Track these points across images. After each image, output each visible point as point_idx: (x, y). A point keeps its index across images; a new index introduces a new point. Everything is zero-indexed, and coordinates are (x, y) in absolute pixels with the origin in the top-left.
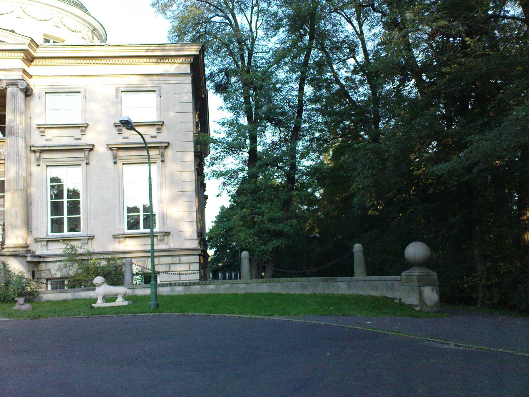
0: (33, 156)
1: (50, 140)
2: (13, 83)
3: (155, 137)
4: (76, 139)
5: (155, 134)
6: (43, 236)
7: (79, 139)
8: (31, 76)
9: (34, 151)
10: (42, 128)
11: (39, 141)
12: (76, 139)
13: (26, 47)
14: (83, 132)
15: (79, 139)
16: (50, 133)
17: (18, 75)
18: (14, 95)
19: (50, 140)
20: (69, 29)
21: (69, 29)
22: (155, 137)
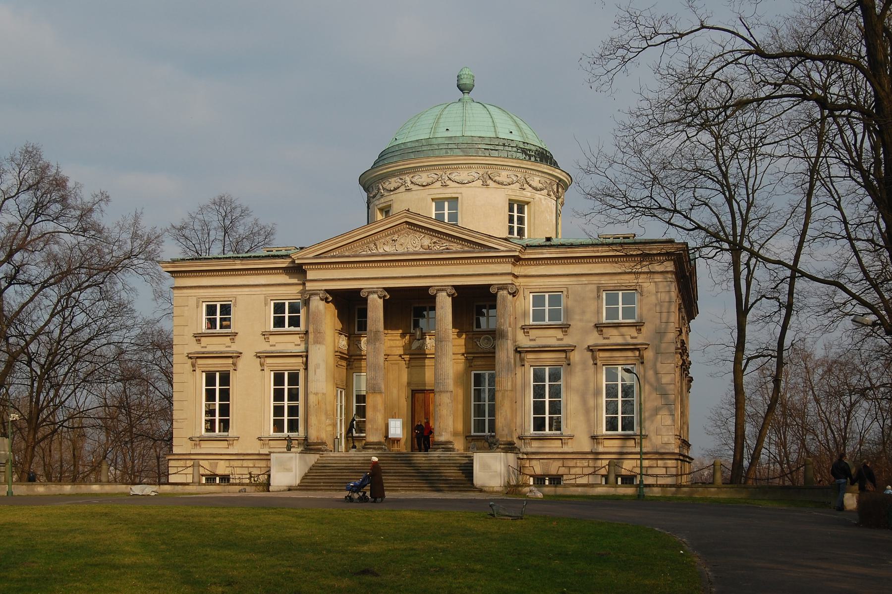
0: (518, 355)
1: (534, 340)
2: (503, 287)
3: (636, 338)
4: (558, 340)
5: (636, 335)
6: (527, 434)
7: (561, 339)
8: (516, 277)
9: (520, 352)
10: (525, 329)
11: (524, 341)
12: (558, 340)
13: (517, 254)
14: (565, 333)
15: (561, 339)
16: (533, 333)
17: (508, 280)
18: (504, 299)
19: (534, 340)
20: (534, 188)
21: (534, 188)
22: (636, 338)
